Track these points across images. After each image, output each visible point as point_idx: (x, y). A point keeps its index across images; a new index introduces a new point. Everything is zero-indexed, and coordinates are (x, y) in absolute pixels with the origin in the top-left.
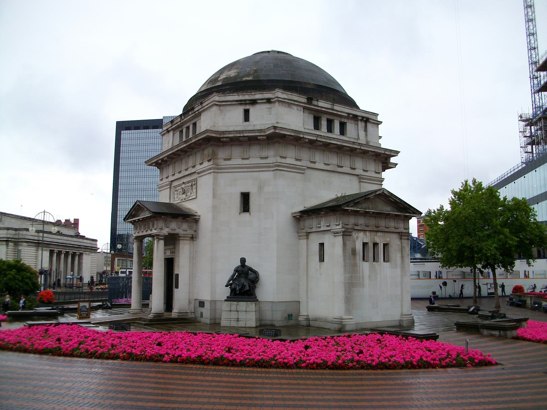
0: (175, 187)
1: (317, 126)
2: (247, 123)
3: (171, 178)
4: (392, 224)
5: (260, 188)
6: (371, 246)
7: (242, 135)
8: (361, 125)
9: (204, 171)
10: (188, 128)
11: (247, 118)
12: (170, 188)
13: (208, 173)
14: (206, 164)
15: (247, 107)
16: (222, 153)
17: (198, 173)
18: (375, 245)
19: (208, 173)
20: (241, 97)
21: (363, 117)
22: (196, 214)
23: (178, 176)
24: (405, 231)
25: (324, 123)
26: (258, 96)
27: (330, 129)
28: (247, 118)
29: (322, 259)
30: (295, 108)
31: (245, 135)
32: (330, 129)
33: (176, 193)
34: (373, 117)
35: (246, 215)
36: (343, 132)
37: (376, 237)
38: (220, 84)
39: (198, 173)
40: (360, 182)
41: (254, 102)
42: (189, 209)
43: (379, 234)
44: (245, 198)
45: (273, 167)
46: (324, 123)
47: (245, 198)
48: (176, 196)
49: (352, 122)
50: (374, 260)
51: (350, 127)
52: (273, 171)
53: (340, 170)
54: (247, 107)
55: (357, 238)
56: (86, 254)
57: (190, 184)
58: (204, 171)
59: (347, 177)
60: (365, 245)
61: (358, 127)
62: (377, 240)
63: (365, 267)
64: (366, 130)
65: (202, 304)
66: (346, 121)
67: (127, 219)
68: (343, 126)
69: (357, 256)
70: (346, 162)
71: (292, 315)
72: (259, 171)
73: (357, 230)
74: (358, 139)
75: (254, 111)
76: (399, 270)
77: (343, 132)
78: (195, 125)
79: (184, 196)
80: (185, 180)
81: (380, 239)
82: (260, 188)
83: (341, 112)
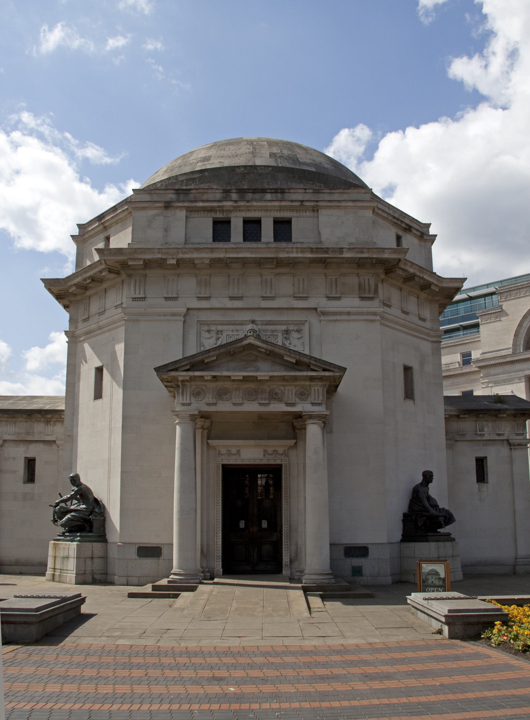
0: (201, 323)
13: (366, 320)
14: (351, 303)
15: (400, 233)
16: (389, 291)
17: (323, 313)
19: (366, 320)
39: (323, 313)
45: (432, 337)
52: (432, 342)
57: (284, 327)
58: (349, 313)
65: (362, 551)
67: (176, 370)
72: (420, 338)
80: (258, 317)
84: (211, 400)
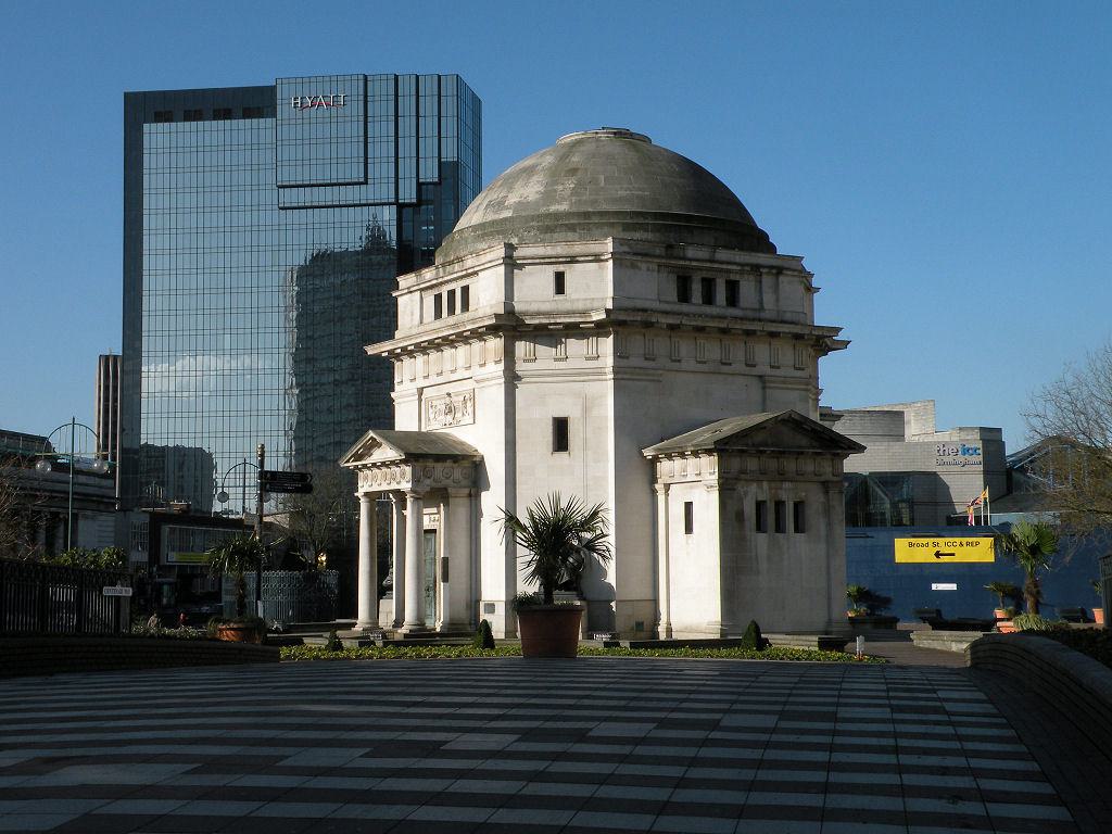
0: (431, 399)
1: (684, 297)
2: (561, 297)
3: (421, 383)
4: (809, 466)
5: (586, 410)
6: (771, 507)
7: (552, 321)
8: (767, 280)
9: (488, 379)
10: (452, 293)
11: (560, 287)
12: (420, 400)
15: (561, 268)
18: (779, 505)
20: (550, 251)
21: (772, 267)
22: (475, 453)
23: (434, 380)
24: (835, 479)
25: (697, 289)
26: (578, 248)
27: (709, 299)
28: (560, 287)
29: (689, 529)
30: (644, 266)
31: (558, 321)
32: (709, 299)
33: (431, 411)
34: (793, 264)
35: (564, 455)
36: (733, 300)
37: (779, 491)
38: (508, 214)
40: (764, 388)
41: (573, 260)
42: (462, 444)
43: (787, 485)
44: (561, 429)
46: (697, 289)
47: (561, 429)
48: (432, 416)
49: (752, 278)
50: (798, 529)
51: (747, 289)
53: (725, 369)
54: (561, 268)
55: (746, 493)
56: (86, 517)
58: (488, 379)
59: (741, 380)
60: (760, 505)
61: (761, 288)
62: (784, 496)
63: (762, 540)
64: (777, 285)
66: (737, 278)
68: (733, 288)
69: (747, 523)
70: (738, 351)
71: (643, 623)
73: (746, 480)
74: (762, 308)
75: (573, 275)
76: (822, 546)
77: (733, 300)
78: (465, 290)
79: (449, 417)
81: (788, 494)
82: (586, 410)
83: (728, 263)
84: (369, 483)
